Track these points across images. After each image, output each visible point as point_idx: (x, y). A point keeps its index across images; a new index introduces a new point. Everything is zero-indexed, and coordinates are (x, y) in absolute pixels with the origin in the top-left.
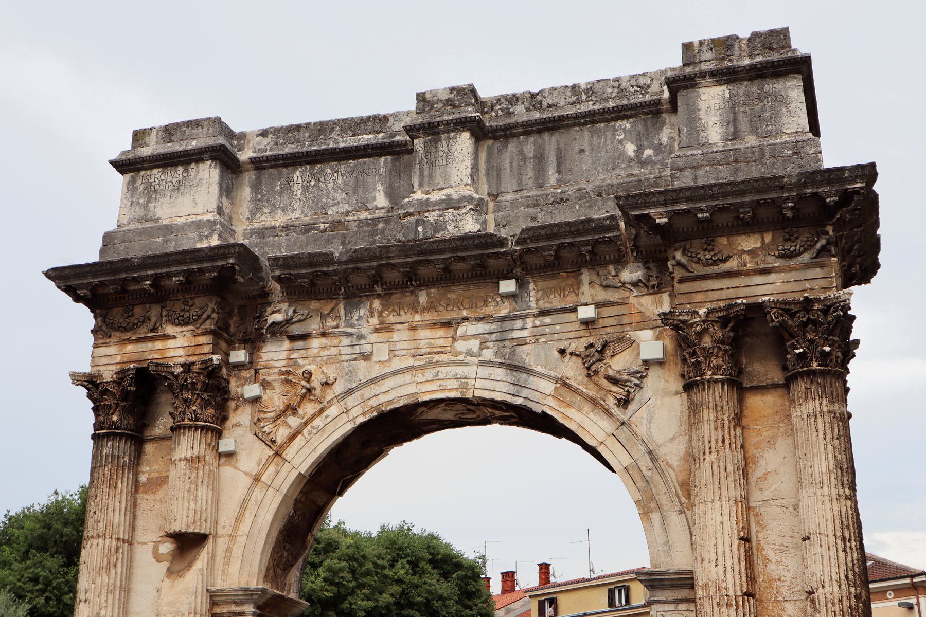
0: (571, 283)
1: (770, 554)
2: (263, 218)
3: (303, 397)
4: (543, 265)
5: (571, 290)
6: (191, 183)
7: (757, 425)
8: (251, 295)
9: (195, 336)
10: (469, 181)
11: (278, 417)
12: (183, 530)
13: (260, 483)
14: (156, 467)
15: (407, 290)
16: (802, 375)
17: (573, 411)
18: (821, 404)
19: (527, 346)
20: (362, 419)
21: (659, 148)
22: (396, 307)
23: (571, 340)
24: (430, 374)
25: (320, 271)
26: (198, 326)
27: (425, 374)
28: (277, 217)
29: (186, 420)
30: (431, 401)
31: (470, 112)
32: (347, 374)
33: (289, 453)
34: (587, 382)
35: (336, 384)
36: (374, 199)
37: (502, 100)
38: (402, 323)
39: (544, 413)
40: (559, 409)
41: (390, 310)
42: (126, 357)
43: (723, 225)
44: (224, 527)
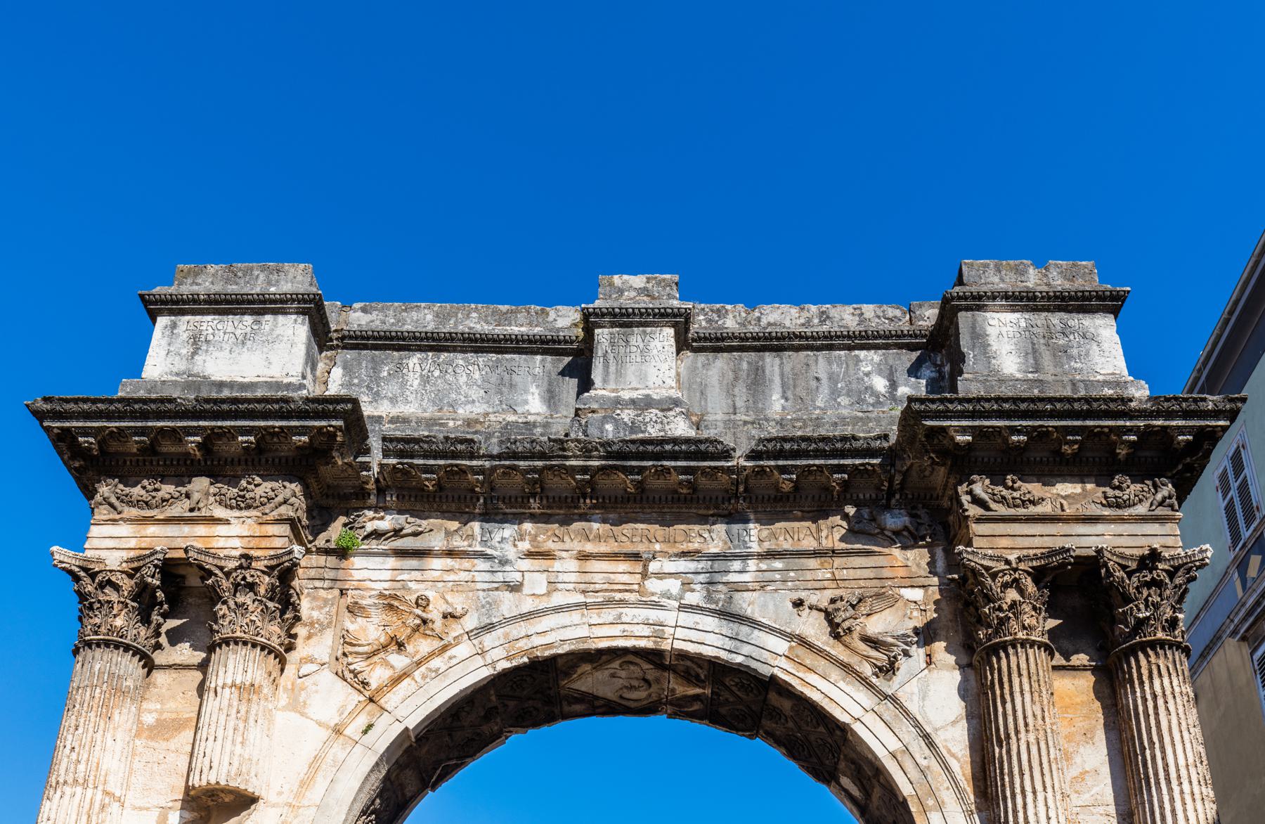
3: (416, 629)
4: (773, 496)
6: (264, 338)
8: (342, 493)
9: (260, 524)
10: (674, 384)
13: (341, 737)
15: (576, 511)
16: (1143, 647)
20: (506, 665)
23: (811, 591)
24: (609, 615)
25: (457, 466)
27: (602, 615)
32: (483, 607)
33: (391, 700)
35: (466, 618)
36: (526, 402)
38: (567, 551)
39: (773, 678)
40: (797, 674)
41: (549, 534)
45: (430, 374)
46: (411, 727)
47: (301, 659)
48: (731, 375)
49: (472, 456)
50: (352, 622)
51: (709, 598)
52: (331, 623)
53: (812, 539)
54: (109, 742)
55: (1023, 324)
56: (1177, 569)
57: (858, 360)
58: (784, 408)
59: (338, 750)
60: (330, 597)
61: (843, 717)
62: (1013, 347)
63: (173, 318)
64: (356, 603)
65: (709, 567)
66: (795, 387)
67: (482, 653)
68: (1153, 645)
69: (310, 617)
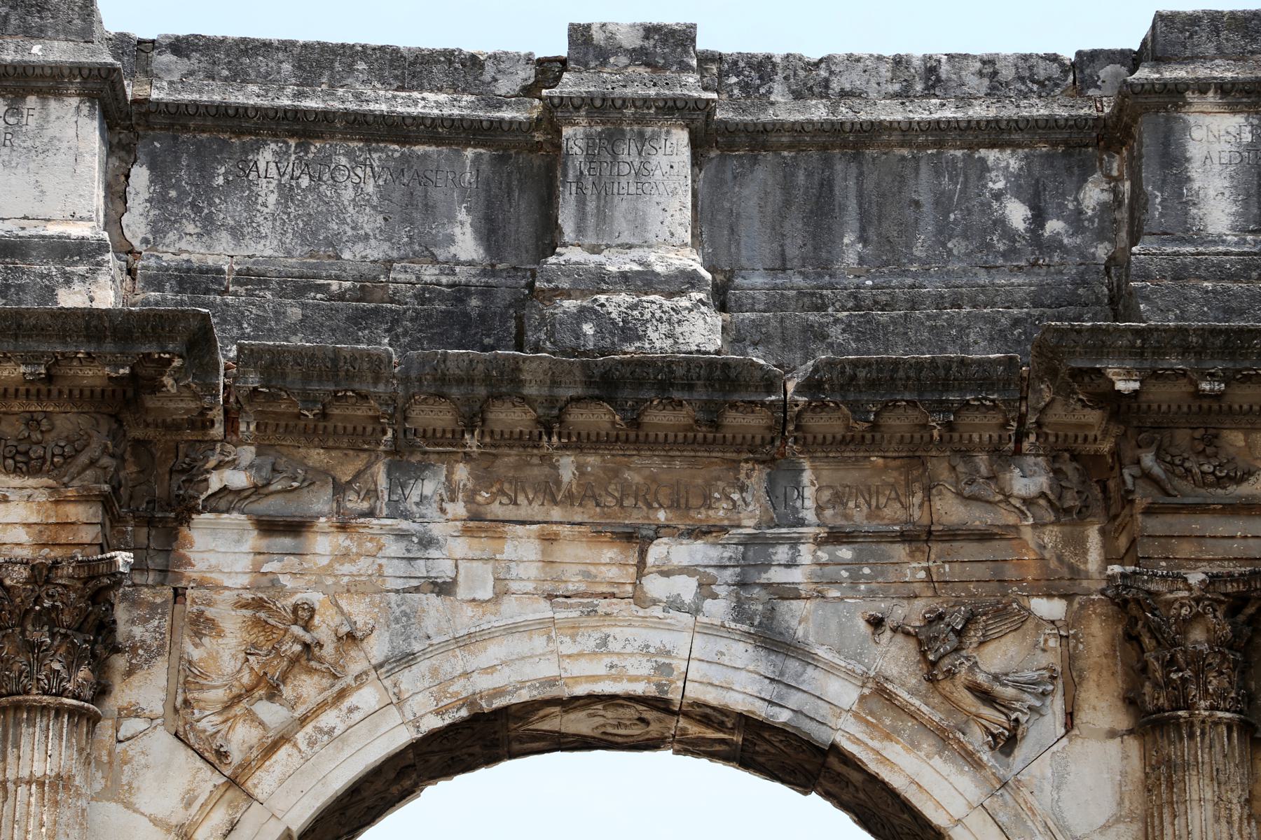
0: (892, 480)
2: (183, 245)
4: (839, 437)
5: (893, 495)
6: (29, 143)
8: (169, 420)
10: (689, 239)
11: (237, 699)
15: (535, 451)
17: (898, 748)
19: (801, 603)
20: (433, 723)
21: (1076, 220)
22: (506, 486)
23: (895, 601)
24: (588, 642)
26: (66, 479)
27: (578, 639)
28: (219, 249)
29: (35, 691)
30: (590, 696)
31: (690, 86)
33: (264, 781)
34: (928, 690)
35: (372, 640)
36: (451, 240)
37: (742, 64)
38: (523, 523)
39: (835, 748)
40: (870, 743)
41: (494, 490)
43: (1241, 407)
45: (293, 183)
47: (120, 710)
48: (778, 196)
50: (196, 645)
51: (740, 612)
52: (162, 646)
53: (899, 505)
58: (861, 260)
60: (158, 600)
61: (937, 818)
65: (740, 556)
66: (880, 218)
67: (399, 702)
69: (131, 637)
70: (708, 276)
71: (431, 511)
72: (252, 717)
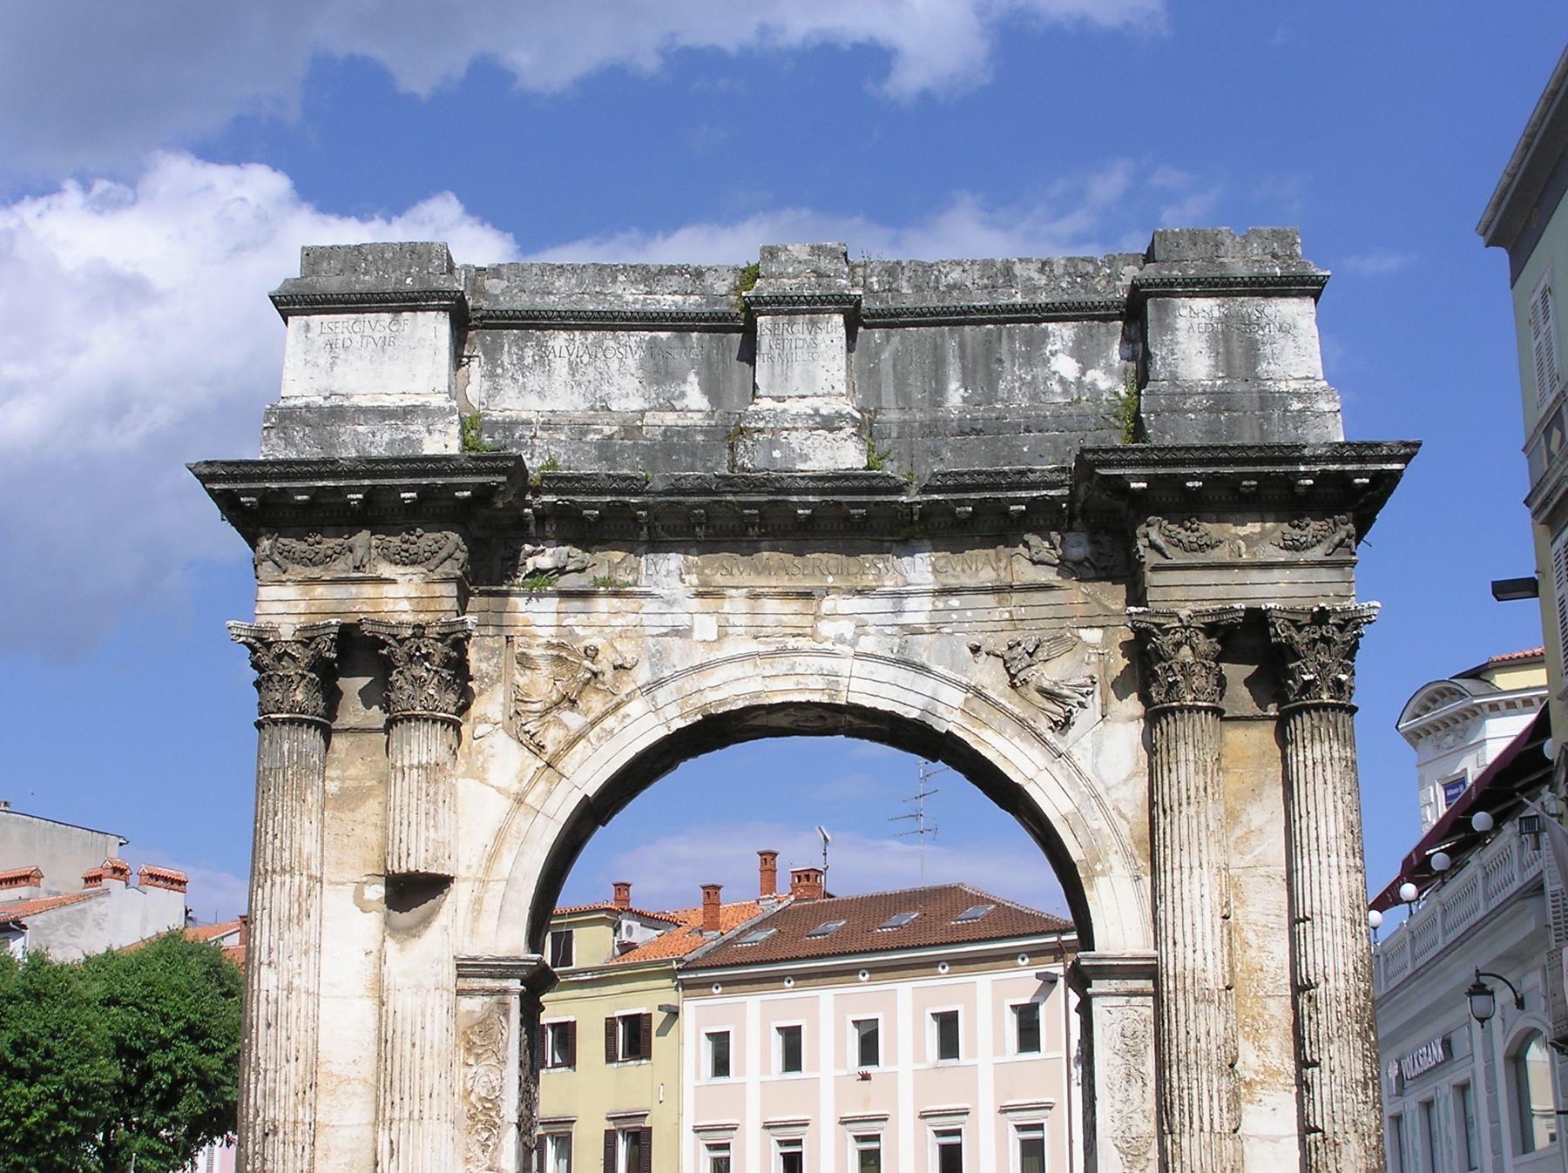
1: (1251, 937)
7: (1238, 768)
11: (547, 711)
12: (421, 871)
14: (352, 771)
16: (1308, 708)
17: (990, 732)
18: (1331, 748)
20: (681, 724)
24: (782, 665)
29: (418, 708)
33: (568, 764)
38: (737, 588)
42: (313, 605)
44: (469, 867)
45: (578, 360)
46: (590, 795)
49: (636, 494)
50: (522, 675)
52: (501, 676)
54: (307, 824)
55: (1216, 314)
56: (1348, 622)
57: (1046, 335)
58: (964, 400)
59: (521, 822)
60: (496, 646)
61: (1015, 777)
62: (1204, 346)
63: (305, 317)
64: (524, 654)
67: (657, 710)
68: (1316, 707)
70: (858, 416)
71: (675, 582)
72: (559, 723)
